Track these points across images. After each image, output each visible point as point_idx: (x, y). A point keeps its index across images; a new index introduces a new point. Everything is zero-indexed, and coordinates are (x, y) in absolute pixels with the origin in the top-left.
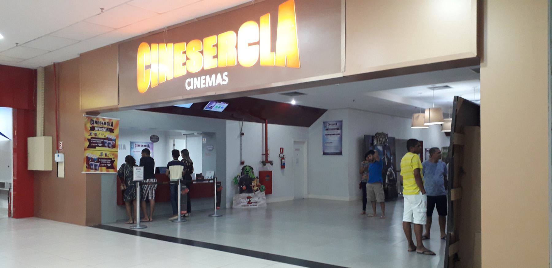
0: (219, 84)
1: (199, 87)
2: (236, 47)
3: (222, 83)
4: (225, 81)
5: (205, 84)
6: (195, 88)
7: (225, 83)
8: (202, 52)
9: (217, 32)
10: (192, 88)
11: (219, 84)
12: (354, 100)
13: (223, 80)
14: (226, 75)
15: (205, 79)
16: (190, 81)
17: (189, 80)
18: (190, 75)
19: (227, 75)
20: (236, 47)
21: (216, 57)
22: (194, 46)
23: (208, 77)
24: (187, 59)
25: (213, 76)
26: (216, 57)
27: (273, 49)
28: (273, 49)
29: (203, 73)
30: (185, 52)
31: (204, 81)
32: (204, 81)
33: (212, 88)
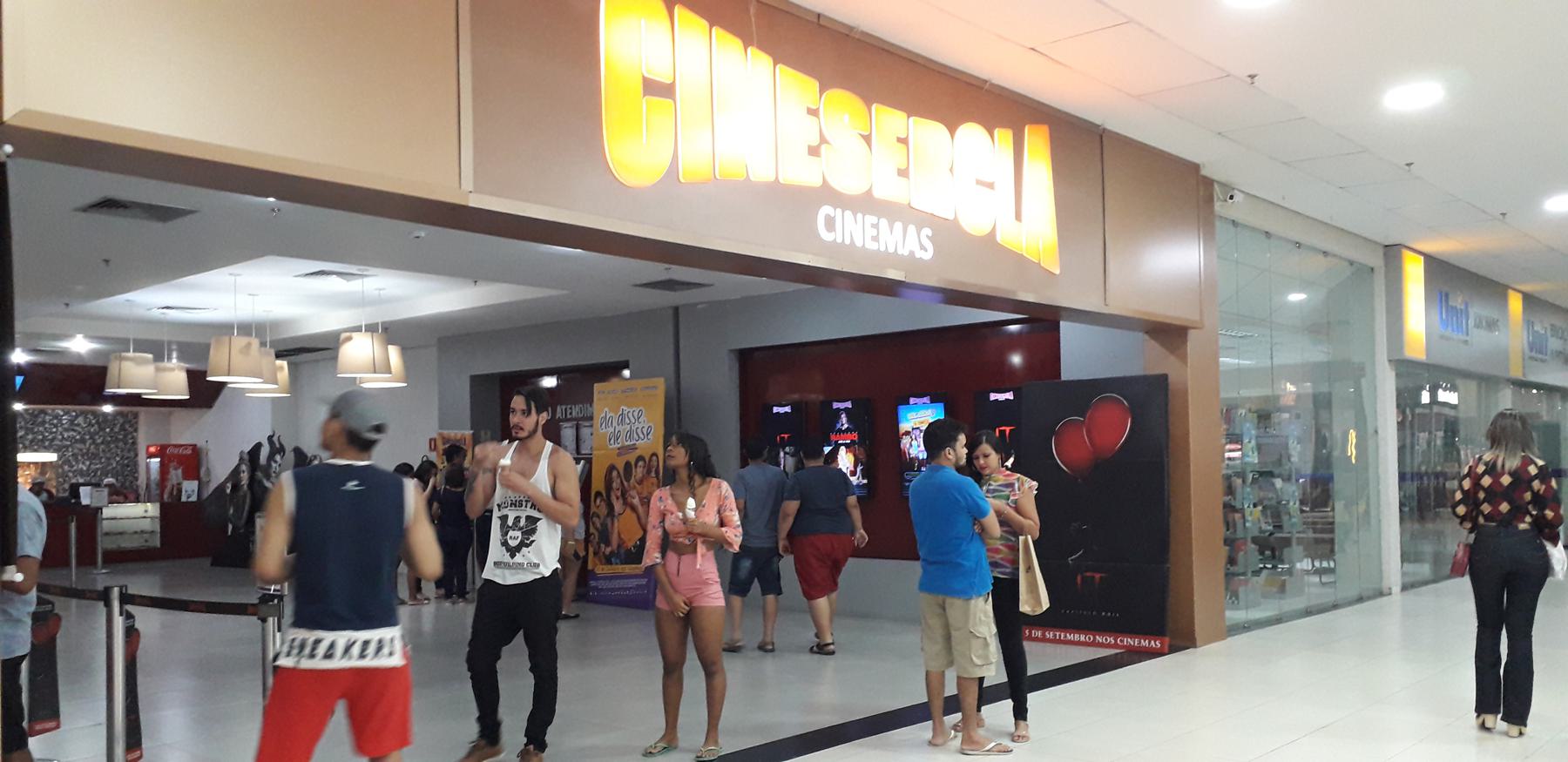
0: (912, 253)
1: (859, 243)
2: (951, 170)
3: (919, 254)
4: (923, 248)
5: (875, 239)
6: (847, 242)
7: (927, 255)
8: (867, 139)
9: (914, 108)
10: (839, 240)
11: (912, 253)
12: (107, 261)
13: (923, 248)
14: (927, 236)
15: (876, 226)
16: (833, 215)
17: (826, 210)
18: (828, 194)
19: (930, 235)
20: (951, 170)
21: (903, 173)
22: (842, 107)
23: (884, 223)
24: (823, 140)
25: (898, 226)
26: (903, 173)
27: (1018, 217)
28: (1018, 217)
29: (865, 204)
30: (813, 112)
31: (874, 232)
32: (874, 232)
33: (894, 259)
